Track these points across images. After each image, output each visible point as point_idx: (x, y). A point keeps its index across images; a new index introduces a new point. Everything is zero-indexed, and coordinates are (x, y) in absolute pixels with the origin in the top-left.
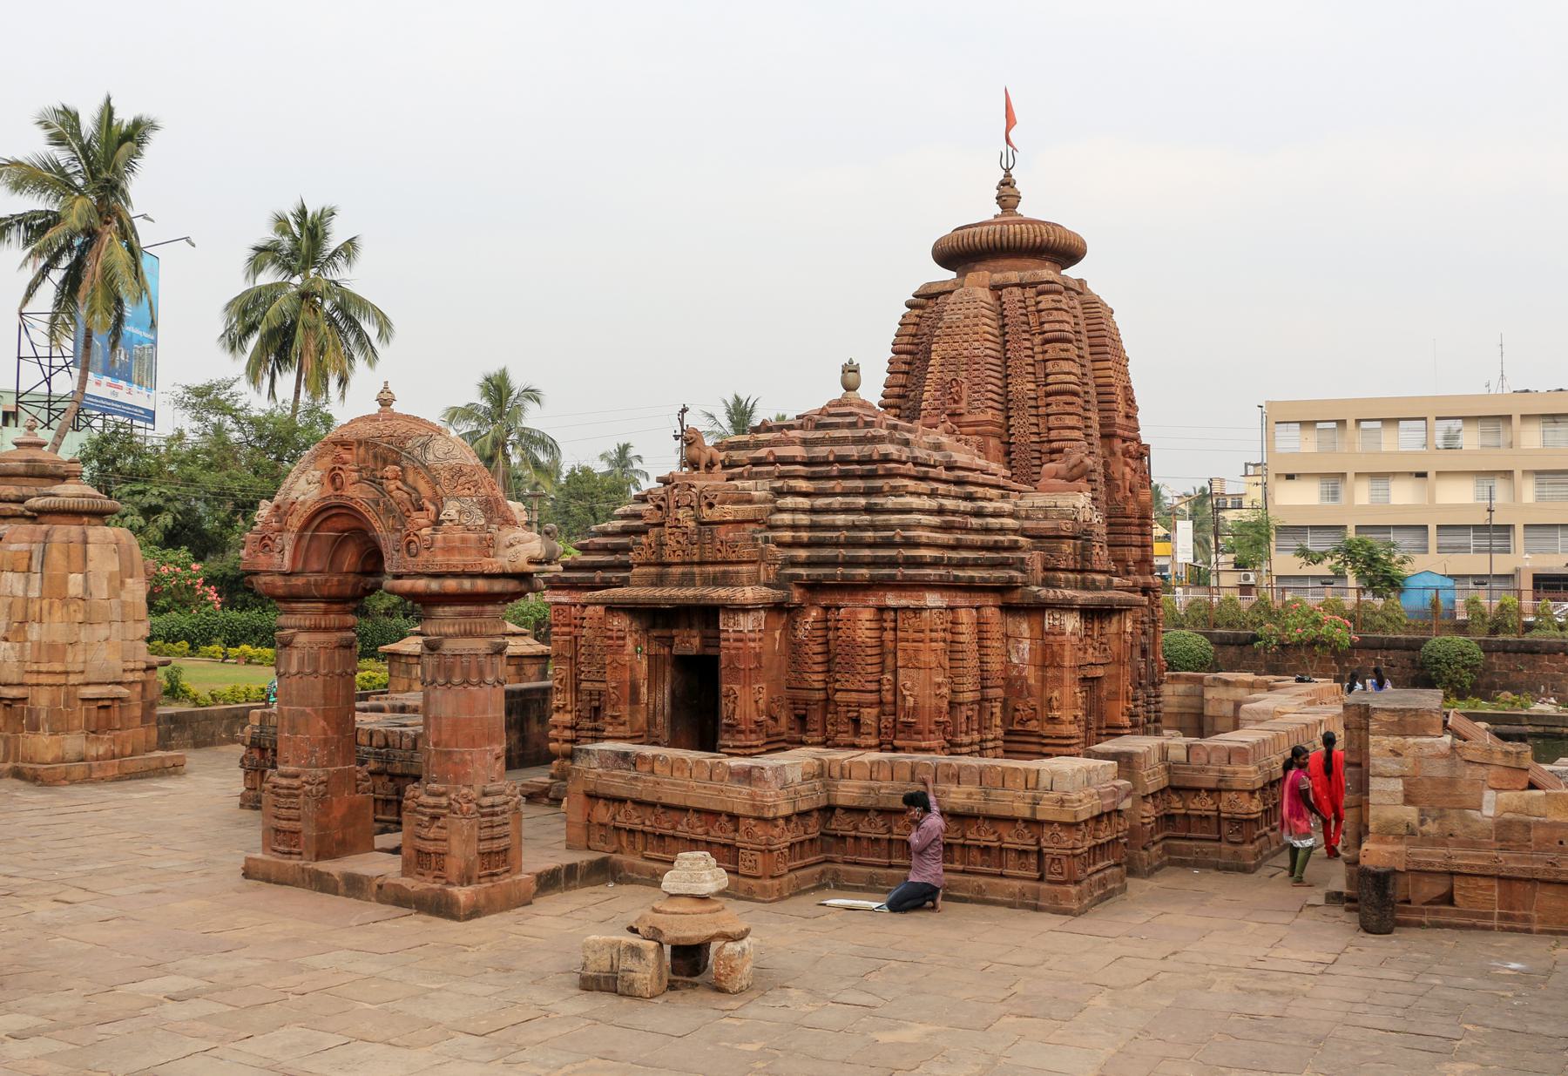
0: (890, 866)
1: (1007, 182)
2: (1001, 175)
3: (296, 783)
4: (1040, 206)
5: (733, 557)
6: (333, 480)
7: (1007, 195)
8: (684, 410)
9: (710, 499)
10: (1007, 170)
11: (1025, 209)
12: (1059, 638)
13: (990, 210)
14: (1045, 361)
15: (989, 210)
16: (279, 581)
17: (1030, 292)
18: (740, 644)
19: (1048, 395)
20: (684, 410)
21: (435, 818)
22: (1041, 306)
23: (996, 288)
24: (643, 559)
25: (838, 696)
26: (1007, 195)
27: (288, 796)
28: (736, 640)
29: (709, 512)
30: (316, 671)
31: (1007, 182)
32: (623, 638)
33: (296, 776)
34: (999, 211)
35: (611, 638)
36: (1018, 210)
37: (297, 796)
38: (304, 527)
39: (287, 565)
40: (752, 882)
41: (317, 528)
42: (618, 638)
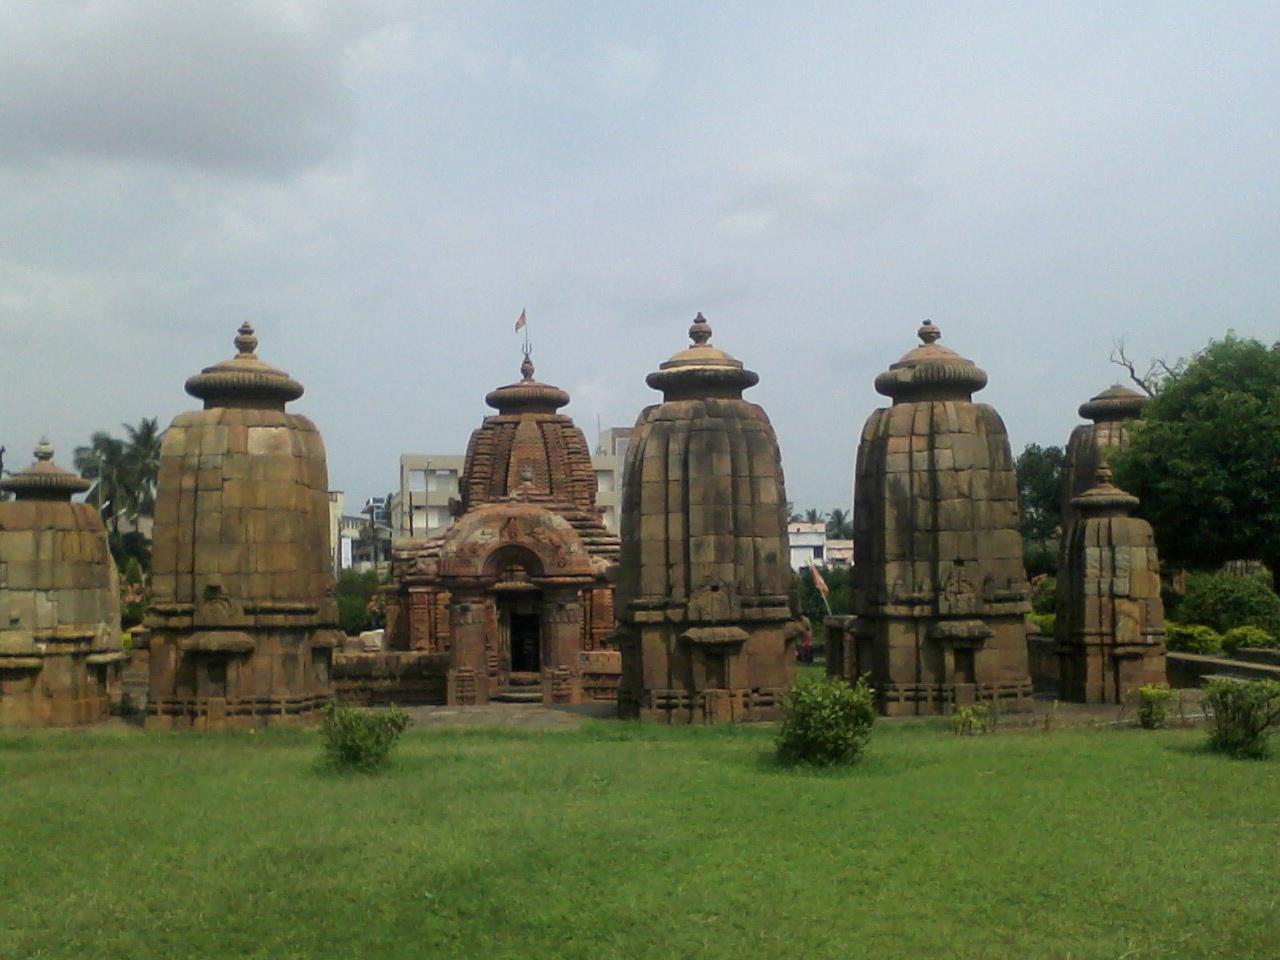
1: (527, 361)
2: (524, 357)
4: (545, 376)
7: (527, 372)
10: (527, 355)
11: (539, 377)
13: (517, 378)
14: (571, 463)
15: (517, 378)
17: (559, 426)
19: (574, 481)
23: (540, 423)
25: (594, 631)
26: (527, 372)
31: (527, 361)
34: (522, 377)
36: (533, 376)
39: (480, 572)
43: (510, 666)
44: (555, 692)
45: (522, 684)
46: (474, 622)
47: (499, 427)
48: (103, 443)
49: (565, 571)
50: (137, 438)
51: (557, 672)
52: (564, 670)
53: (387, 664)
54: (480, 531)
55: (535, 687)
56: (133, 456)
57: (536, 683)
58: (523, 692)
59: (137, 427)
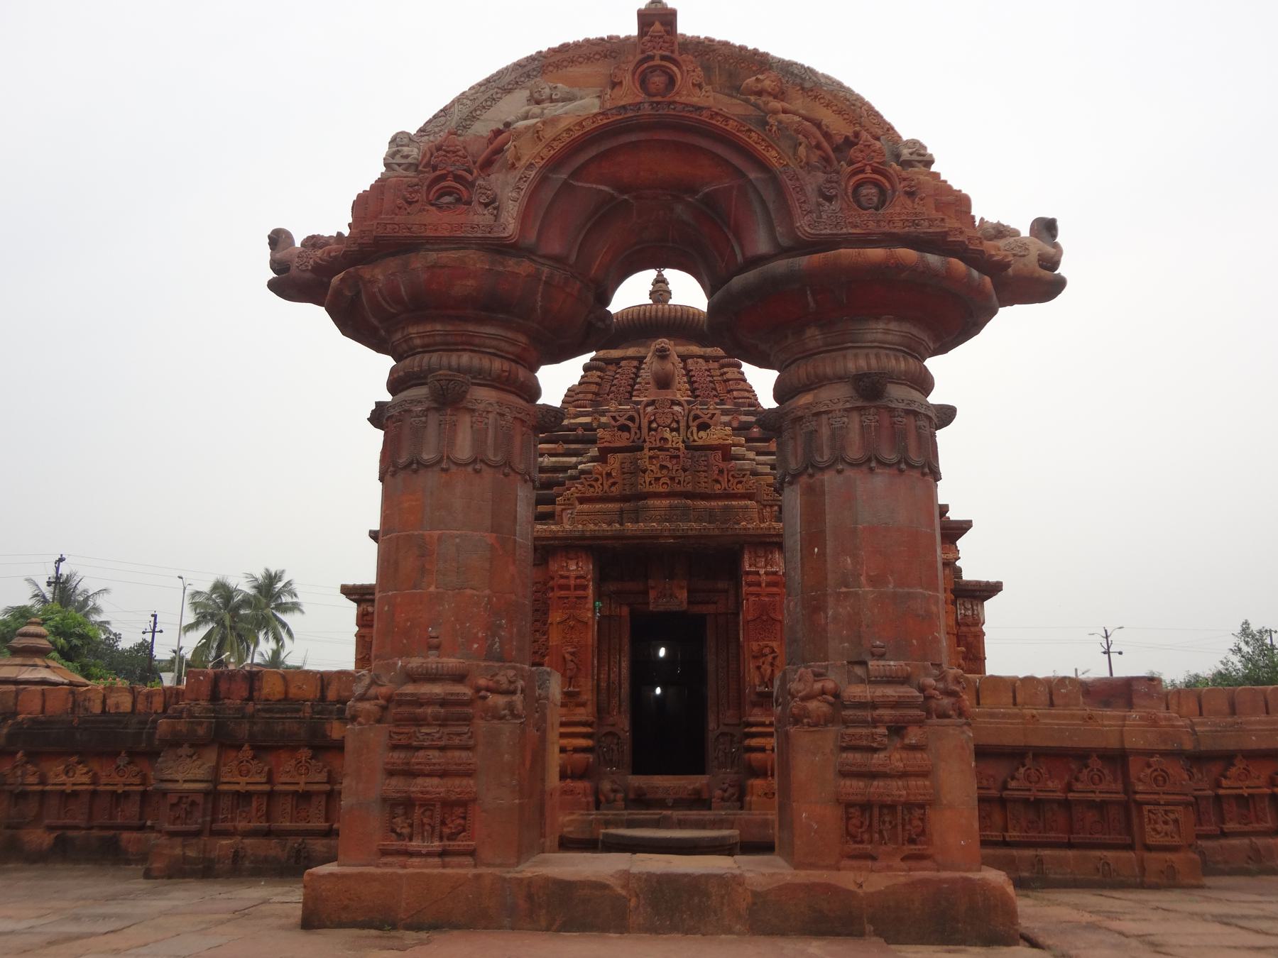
0: (1224, 835)
3: (464, 690)
5: (740, 489)
6: (643, 83)
8: (61, 560)
9: (706, 418)
12: (973, 629)
16: (476, 261)
17: (716, 365)
18: (775, 590)
20: (61, 560)
21: (897, 730)
22: (729, 376)
24: (597, 491)
27: (443, 722)
28: (768, 585)
29: (702, 434)
30: (508, 463)
32: (585, 588)
33: (459, 678)
35: (567, 588)
37: (467, 719)
38: (555, 163)
39: (509, 224)
40: (1168, 856)
41: (575, 174)
42: (577, 587)
43: (627, 748)
44: (854, 787)
45: (662, 804)
46: (477, 460)
47: (612, 368)
48: (222, 589)
49: (897, 214)
50: (258, 588)
51: (858, 691)
52: (891, 680)
53: (214, 697)
54: (521, 95)
55: (693, 814)
56: (247, 602)
57: (699, 801)
58: (657, 824)
59: (259, 574)
